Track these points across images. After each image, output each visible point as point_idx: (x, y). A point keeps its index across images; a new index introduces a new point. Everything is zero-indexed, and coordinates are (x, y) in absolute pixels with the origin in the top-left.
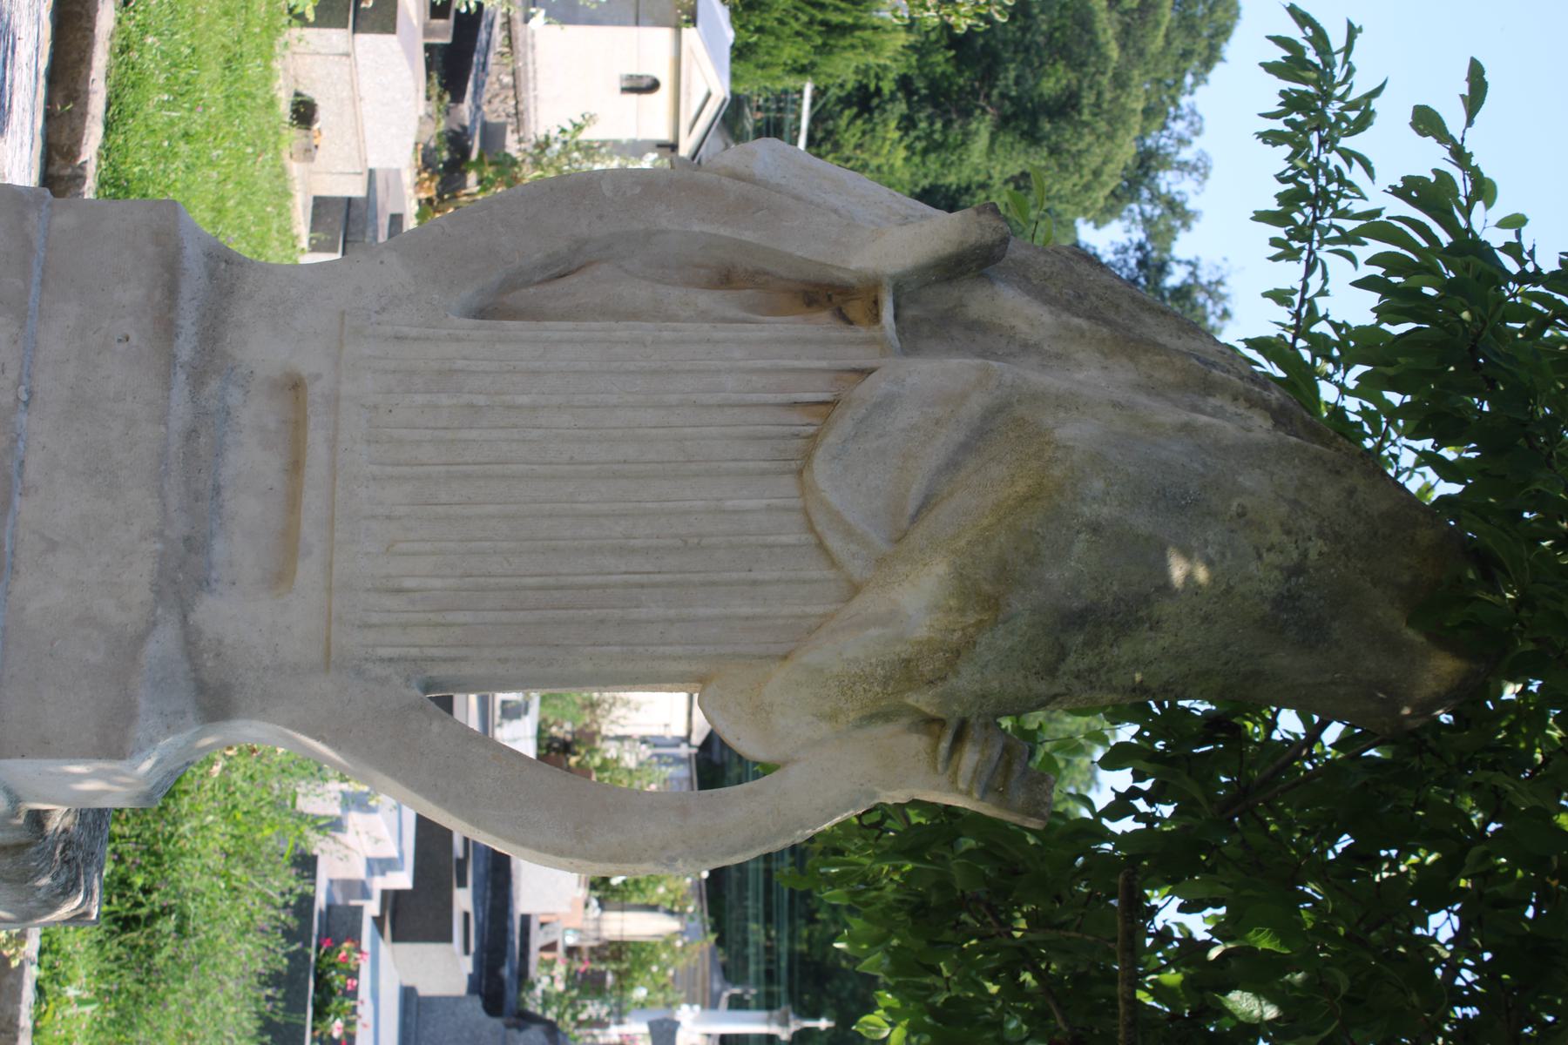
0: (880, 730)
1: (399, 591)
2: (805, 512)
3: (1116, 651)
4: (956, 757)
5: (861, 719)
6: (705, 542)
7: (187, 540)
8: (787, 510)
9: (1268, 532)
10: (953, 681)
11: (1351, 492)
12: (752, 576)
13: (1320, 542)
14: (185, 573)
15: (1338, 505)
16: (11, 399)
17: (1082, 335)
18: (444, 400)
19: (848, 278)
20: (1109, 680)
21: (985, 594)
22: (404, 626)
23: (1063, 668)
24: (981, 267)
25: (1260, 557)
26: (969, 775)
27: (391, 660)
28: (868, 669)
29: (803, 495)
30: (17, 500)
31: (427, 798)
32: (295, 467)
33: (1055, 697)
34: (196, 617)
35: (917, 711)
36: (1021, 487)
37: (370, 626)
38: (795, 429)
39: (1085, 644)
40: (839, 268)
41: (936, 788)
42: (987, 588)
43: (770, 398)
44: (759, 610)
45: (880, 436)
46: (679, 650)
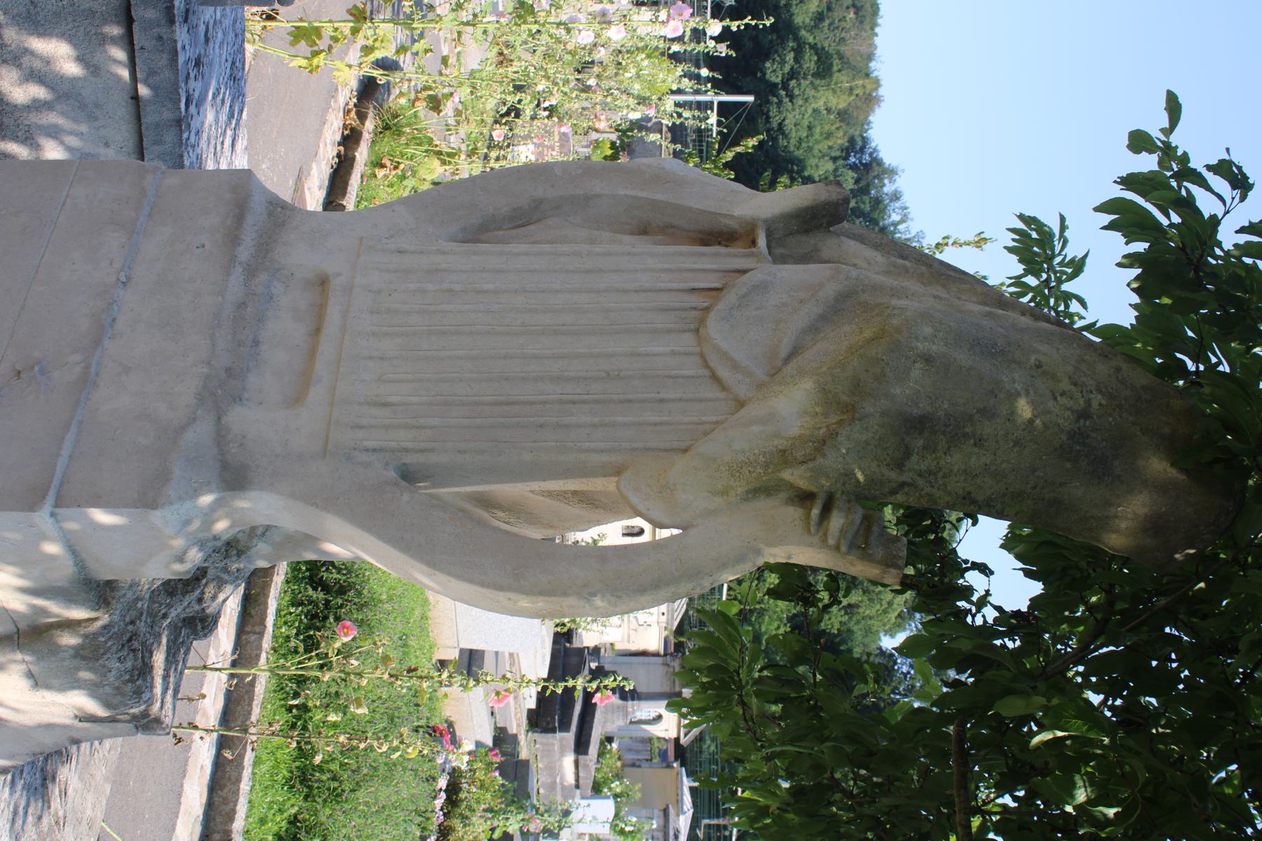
0: (764, 505)
1: (385, 405)
2: (702, 355)
3: (949, 459)
4: (825, 523)
5: (748, 492)
6: (623, 373)
7: (228, 370)
8: (686, 354)
9: (1059, 381)
10: (820, 461)
11: (1118, 370)
12: (662, 396)
13: (1099, 397)
14: (224, 389)
15: (1109, 375)
16: (113, 279)
17: (907, 271)
18: (430, 287)
19: (733, 224)
20: (945, 485)
21: (844, 402)
22: (386, 427)
23: (908, 465)
24: (831, 224)
25: (1055, 399)
26: (837, 534)
27: (374, 450)
28: (752, 458)
29: (700, 344)
30: (106, 342)
31: (394, 547)
32: (317, 331)
33: (903, 485)
34: (225, 420)
35: (791, 486)
36: (868, 334)
37: (361, 427)
38: (693, 305)
39: (924, 448)
40: (725, 216)
41: (811, 545)
42: (845, 398)
43: (675, 286)
44: (665, 419)
45: (758, 308)
46: (602, 445)
